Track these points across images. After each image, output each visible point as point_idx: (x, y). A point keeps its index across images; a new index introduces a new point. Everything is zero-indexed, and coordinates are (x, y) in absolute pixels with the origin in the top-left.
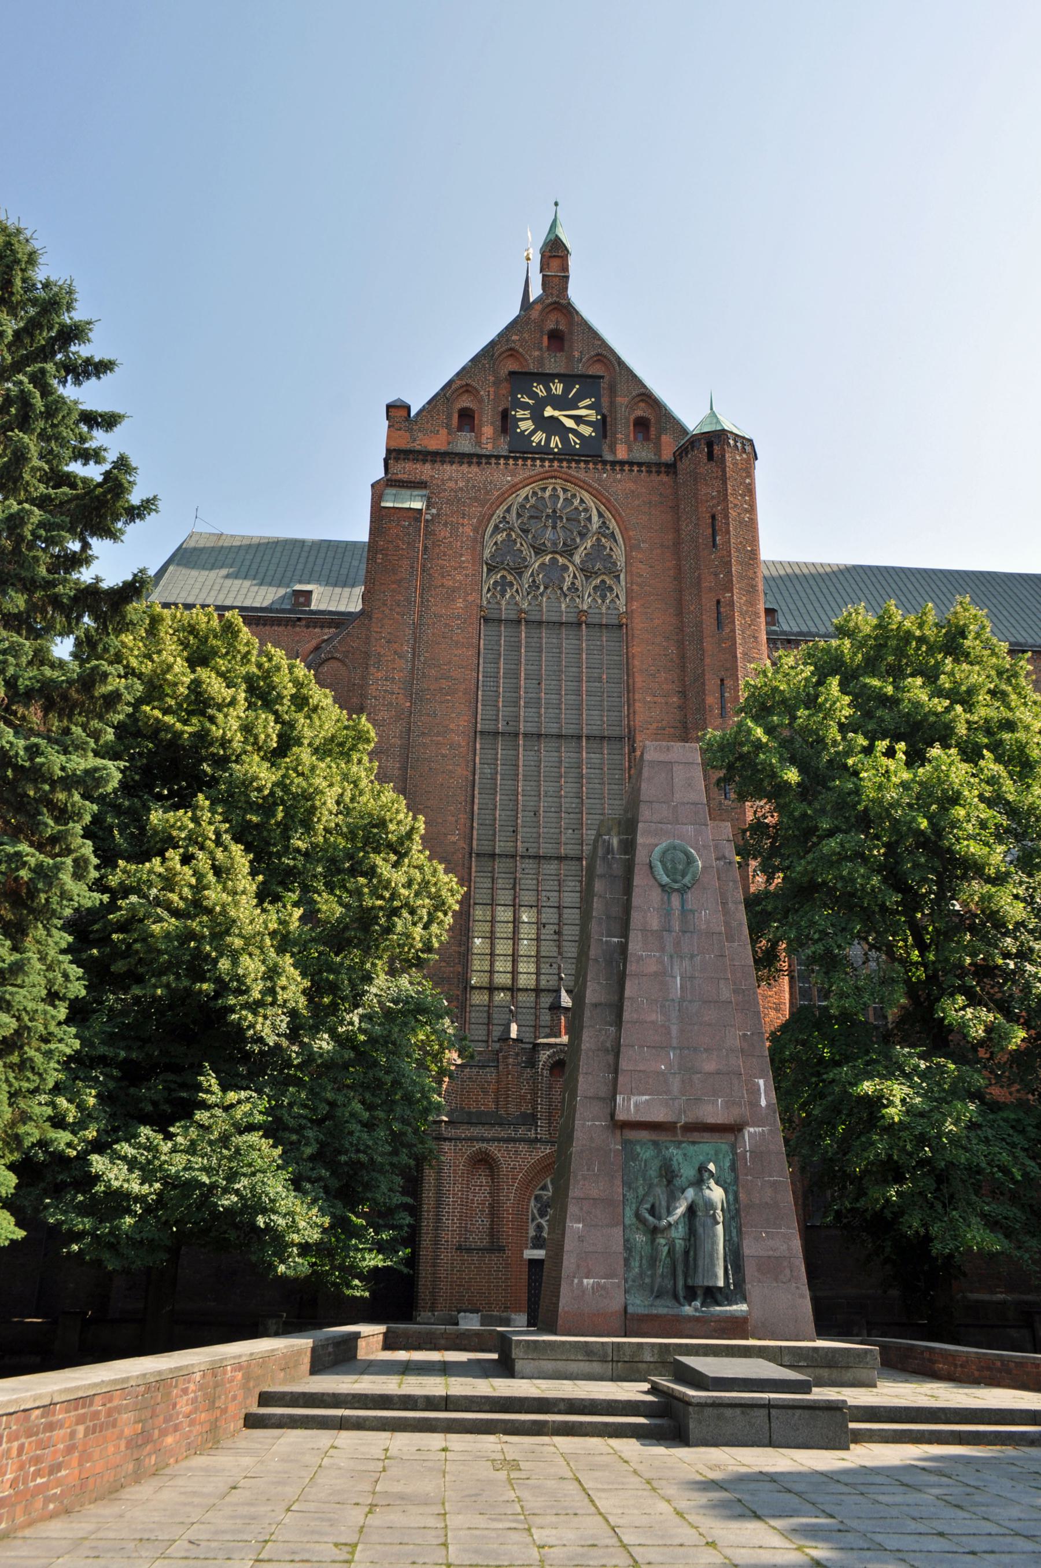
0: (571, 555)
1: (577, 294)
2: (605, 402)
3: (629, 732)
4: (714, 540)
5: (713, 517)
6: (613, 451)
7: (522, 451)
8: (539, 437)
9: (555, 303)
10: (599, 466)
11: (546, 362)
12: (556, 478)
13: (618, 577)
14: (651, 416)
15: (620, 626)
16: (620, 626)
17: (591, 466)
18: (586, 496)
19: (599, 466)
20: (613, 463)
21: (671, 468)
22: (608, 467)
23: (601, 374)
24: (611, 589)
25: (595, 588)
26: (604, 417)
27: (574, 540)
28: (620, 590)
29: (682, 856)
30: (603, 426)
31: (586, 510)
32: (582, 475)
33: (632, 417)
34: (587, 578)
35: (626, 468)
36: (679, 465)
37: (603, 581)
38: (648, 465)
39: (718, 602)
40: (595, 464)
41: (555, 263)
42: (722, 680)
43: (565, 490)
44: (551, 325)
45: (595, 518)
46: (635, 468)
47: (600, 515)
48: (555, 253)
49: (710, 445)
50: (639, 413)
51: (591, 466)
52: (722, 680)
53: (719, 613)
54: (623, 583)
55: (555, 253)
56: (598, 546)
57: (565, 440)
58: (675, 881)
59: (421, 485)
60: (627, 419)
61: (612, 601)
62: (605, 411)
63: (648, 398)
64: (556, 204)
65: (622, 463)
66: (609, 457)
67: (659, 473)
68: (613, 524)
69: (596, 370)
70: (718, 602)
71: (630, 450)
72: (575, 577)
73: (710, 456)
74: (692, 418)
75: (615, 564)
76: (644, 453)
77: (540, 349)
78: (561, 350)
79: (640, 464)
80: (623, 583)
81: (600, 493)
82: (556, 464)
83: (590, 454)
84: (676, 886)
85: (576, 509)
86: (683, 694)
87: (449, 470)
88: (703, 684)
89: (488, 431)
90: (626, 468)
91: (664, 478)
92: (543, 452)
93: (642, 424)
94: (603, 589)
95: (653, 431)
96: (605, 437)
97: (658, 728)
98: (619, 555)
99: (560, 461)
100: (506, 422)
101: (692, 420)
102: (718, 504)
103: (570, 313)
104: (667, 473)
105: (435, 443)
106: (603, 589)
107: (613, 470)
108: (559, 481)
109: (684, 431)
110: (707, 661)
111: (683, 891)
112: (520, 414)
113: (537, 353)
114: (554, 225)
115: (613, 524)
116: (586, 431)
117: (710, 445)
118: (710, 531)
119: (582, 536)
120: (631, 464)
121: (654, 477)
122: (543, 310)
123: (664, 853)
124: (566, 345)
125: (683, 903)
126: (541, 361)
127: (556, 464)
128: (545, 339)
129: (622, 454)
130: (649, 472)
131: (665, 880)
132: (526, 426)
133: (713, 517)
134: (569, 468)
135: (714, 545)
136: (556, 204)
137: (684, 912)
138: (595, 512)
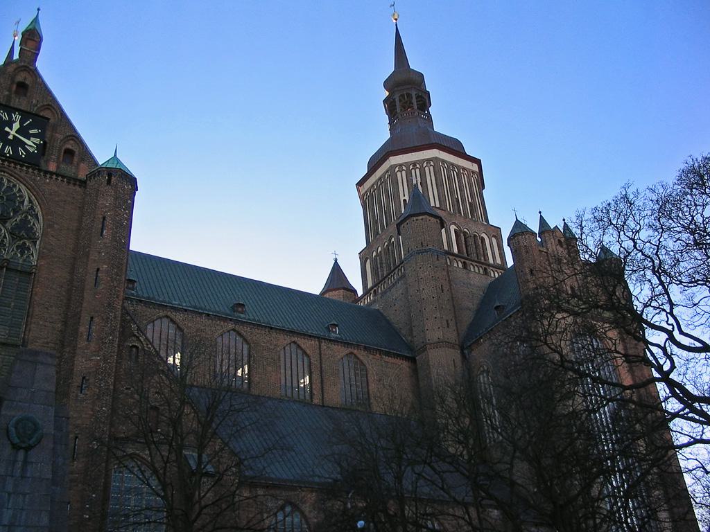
0: (5, 222)
2: (48, 134)
3: (24, 342)
4: (102, 232)
5: (104, 218)
6: (47, 162)
9: (26, 66)
10: (36, 172)
11: (13, 100)
12: (4, 172)
13: (35, 243)
14: (75, 149)
15: (30, 274)
16: (30, 274)
17: (30, 170)
18: (23, 188)
19: (36, 172)
20: (46, 172)
21: (83, 183)
22: (42, 174)
24: (29, 249)
25: (18, 247)
26: (45, 143)
27: (9, 213)
28: (34, 252)
29: (30, 425)
30: (42, 148)
31: (21, 196)
32: (23, 174)
33: (63, 148)
34: (13, 239)
35: (54, 177)
36: (88, 182)
37: (24, 243)
38: (69, 179)
39: (98, 270)
40: (34, 169)
41: (30, 43)
42: (92, 318)
43: (9, 181)
44: (19, 78)
45: (26, 203)
46: (60, 179)
47: (30, 201)
48: (32, 38)
49: (110, 176)
50: (69, 146)
51: (30, 170)
52: (92, 318)
53: (97, 276)
54: (37, 247)
55: (32, 38)
56: (25, 221)
57: (15, 151)
58: (24, 442)
60: (60, 150)
61: (28, 257)
62: (46, 140)
63: (75, 137)
64: (39, 10)
65: (52, 173)
66: (44, 168)
67: (75, 184)
68: (38, 209)
69: (46, 114)
70: (98, 270)
71: (58, 167)
72: (5, 237)
73: (109, 182)
74: (102, 157)
75: (35, 234)
76: (69, 170)
77: (10, 90)
78: (25, 95)
79: (63, 177)
80: (37, 247)
81: (33, 188)
82: (6, 163)
83: (33, 162)
84: (23, 445)
85: (15, 194)
86: (65, 323)
88: (79, 318)
90: (54, 177)
91: (77, 188)
93: (69, 153)
94: (23, 248)
95: (76, 159)
96: (43, 155)
97: (44, 343)
98: (39, 229)
99: (10, 162)
101: (102, 157)
102: (109, 211)
103: (36, 77)
104: (80, 186)
106: (23, 248)
107: (45, 176)
108: (6, 174)
109: (96, 163)
110: (85, 305)
111: (27, 449)
113: (7, 93)
114: (36, 20)
115: (38, 209)
117: (110, 176)
118: (101, 226)
119: (16, 212)
120: (58, 175)
121: (71, 186)
122: (15, 69)
123: (17, 423)
124: (28, 94)
125: (26, 457)
126: (9, 98)
127: (6, 163)
128: (15, 86)
130: (69, 183)
131: (16, 440)
133: (104, 218)
134: (15, 168)
135: (102, 235)
136: (39, 10)
137: (25, 462)
138: (27, 198)
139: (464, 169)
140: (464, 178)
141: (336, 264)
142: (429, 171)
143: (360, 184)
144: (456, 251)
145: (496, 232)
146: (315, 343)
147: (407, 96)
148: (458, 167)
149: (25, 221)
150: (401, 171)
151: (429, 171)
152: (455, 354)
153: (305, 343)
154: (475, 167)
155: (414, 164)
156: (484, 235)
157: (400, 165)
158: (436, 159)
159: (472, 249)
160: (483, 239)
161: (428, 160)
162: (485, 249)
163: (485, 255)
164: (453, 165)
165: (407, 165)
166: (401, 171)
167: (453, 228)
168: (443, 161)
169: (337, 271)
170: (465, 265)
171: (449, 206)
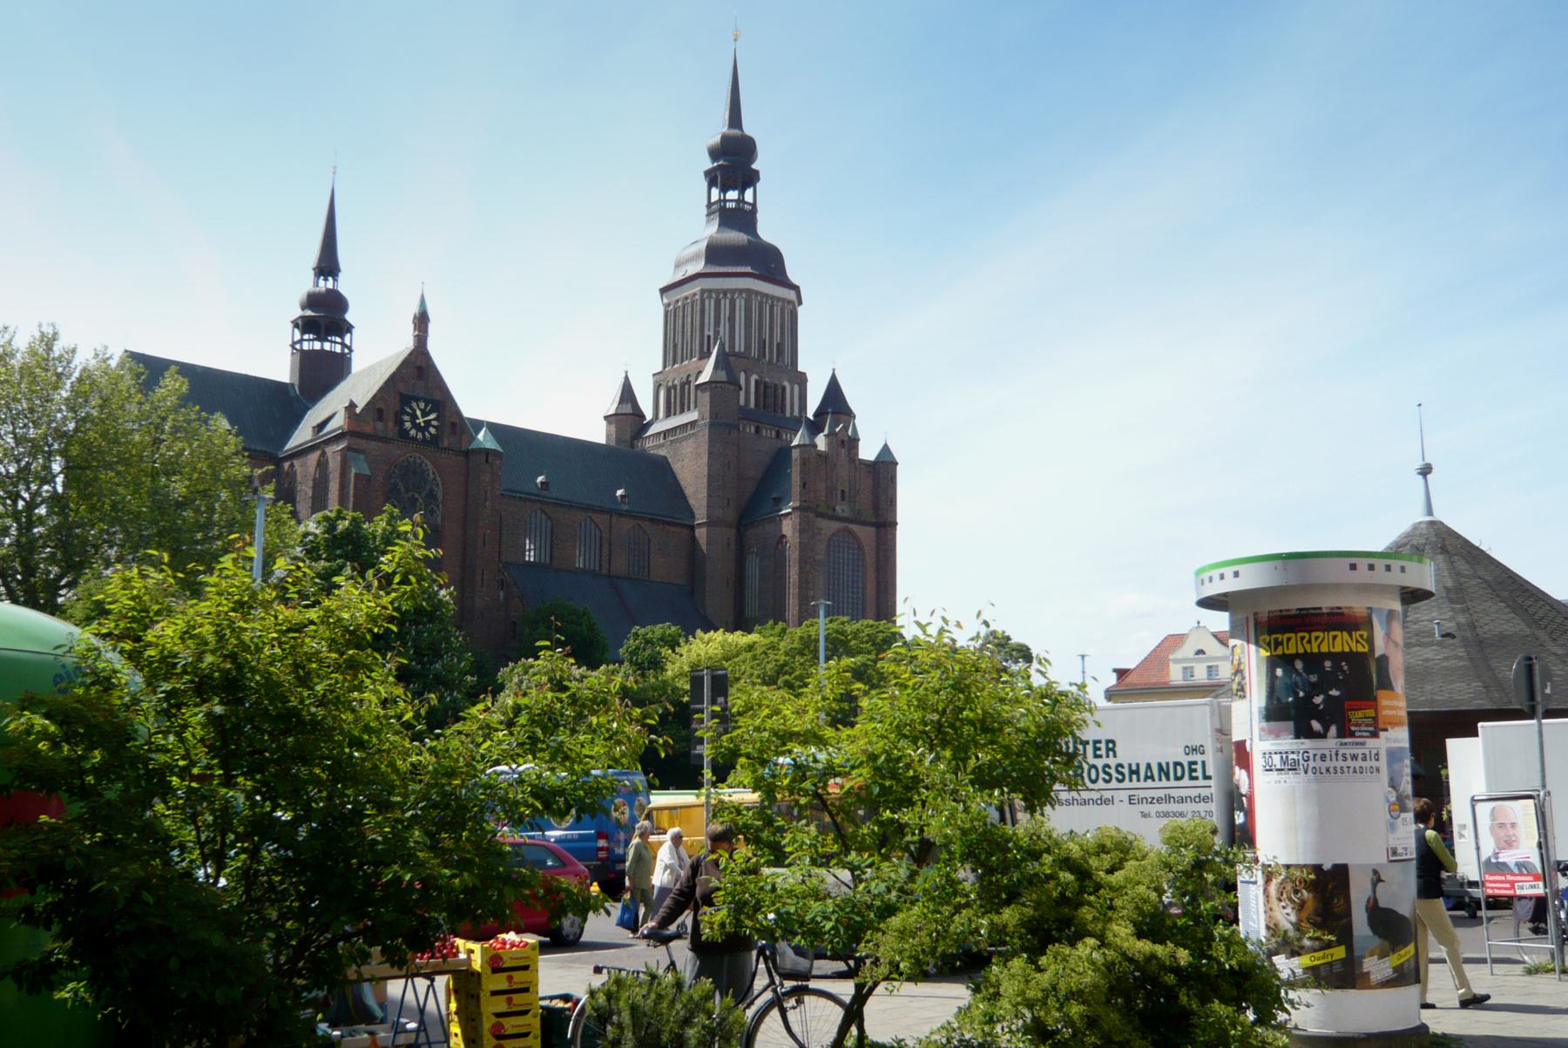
1: (433, 347)
7: (404, 434)
8: (413, 432)
23: (441, 401)
55: (422, 321)
59: (362, 452)
87: (373, 444)
89: (391, 424)
92: (415, 439)
98: (440, 496)
100: (400, 423)
105: (368, 429)
112: (406, 418)
116: (432, 430)
129: (446, 444)
132: (408, 425)
139: (779, 299)
140: (777, 310)
141: (627, 378)
142: (740, 303)
143: (664, 291)
144: (752, 405)
145: (802, 380)
146: (606, 517)
147: (734, 163)
148: (773, 297)
149: (432, 490)
150: (710, 297)
151: (740, 303)
152: (732, 533)
153: (598, 518)
154: (791, 295)
155: (725, 292)
156: (786, 384)
157: (710, 291)
158: (749, 292)
159: (770, 401)
160: (784, 388)
161: (741, 291)
162: (784, 399)
163: (783, 406)
164: (766, 295)
165: (718, 291)
166: (710, 297)
167: (754, 378)
168: (757, 293)
169: (627, 394)
170: (758, 430)
171: (754, 353)
